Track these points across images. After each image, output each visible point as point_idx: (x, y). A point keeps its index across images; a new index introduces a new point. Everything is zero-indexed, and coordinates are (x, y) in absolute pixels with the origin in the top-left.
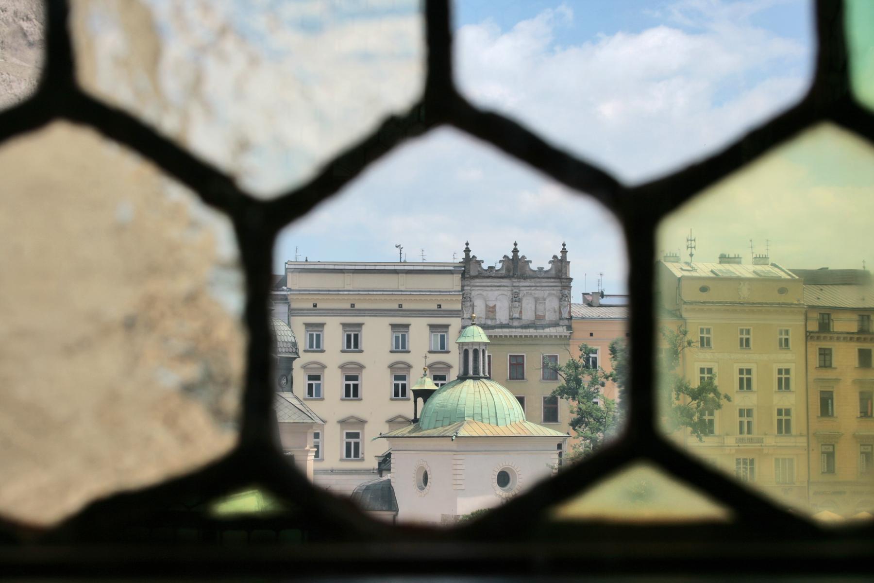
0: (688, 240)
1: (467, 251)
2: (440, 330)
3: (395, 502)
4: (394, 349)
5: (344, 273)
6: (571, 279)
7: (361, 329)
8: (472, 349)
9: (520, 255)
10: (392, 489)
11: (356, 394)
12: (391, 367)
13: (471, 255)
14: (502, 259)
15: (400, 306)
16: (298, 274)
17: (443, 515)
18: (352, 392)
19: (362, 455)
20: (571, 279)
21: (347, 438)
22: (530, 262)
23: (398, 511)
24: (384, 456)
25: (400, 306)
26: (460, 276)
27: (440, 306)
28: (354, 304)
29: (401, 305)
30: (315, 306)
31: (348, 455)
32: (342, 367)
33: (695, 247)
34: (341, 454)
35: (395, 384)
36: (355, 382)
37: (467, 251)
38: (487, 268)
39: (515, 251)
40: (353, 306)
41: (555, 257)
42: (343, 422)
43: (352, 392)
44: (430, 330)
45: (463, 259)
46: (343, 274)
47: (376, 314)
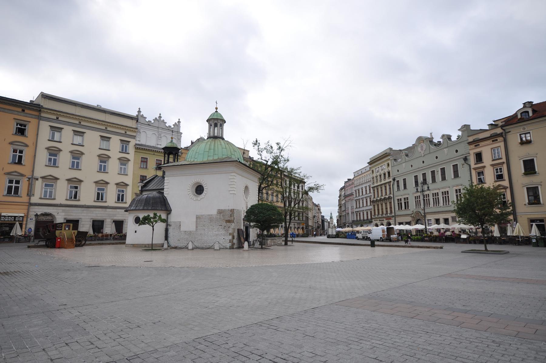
1: (139, 112)
2: (125, 143)
3: (168, 205)
5: (76, 106)
6: (181, 133)
9: (162, 119)
10: (165, 198)
12: (99, 156)
13: (141, 113)
15: (106, 128)
16: (48, 100)
18: (75, 166)
20: (181, 133)
22: (166, 123)
26: (136, 121)
27: (126, 132)
28: (81, 122)
36: (78, 161)
38: (147, 121)
39: (160, 117)
41: (176, 123)
43: (75, 166)
46: (75, 107)
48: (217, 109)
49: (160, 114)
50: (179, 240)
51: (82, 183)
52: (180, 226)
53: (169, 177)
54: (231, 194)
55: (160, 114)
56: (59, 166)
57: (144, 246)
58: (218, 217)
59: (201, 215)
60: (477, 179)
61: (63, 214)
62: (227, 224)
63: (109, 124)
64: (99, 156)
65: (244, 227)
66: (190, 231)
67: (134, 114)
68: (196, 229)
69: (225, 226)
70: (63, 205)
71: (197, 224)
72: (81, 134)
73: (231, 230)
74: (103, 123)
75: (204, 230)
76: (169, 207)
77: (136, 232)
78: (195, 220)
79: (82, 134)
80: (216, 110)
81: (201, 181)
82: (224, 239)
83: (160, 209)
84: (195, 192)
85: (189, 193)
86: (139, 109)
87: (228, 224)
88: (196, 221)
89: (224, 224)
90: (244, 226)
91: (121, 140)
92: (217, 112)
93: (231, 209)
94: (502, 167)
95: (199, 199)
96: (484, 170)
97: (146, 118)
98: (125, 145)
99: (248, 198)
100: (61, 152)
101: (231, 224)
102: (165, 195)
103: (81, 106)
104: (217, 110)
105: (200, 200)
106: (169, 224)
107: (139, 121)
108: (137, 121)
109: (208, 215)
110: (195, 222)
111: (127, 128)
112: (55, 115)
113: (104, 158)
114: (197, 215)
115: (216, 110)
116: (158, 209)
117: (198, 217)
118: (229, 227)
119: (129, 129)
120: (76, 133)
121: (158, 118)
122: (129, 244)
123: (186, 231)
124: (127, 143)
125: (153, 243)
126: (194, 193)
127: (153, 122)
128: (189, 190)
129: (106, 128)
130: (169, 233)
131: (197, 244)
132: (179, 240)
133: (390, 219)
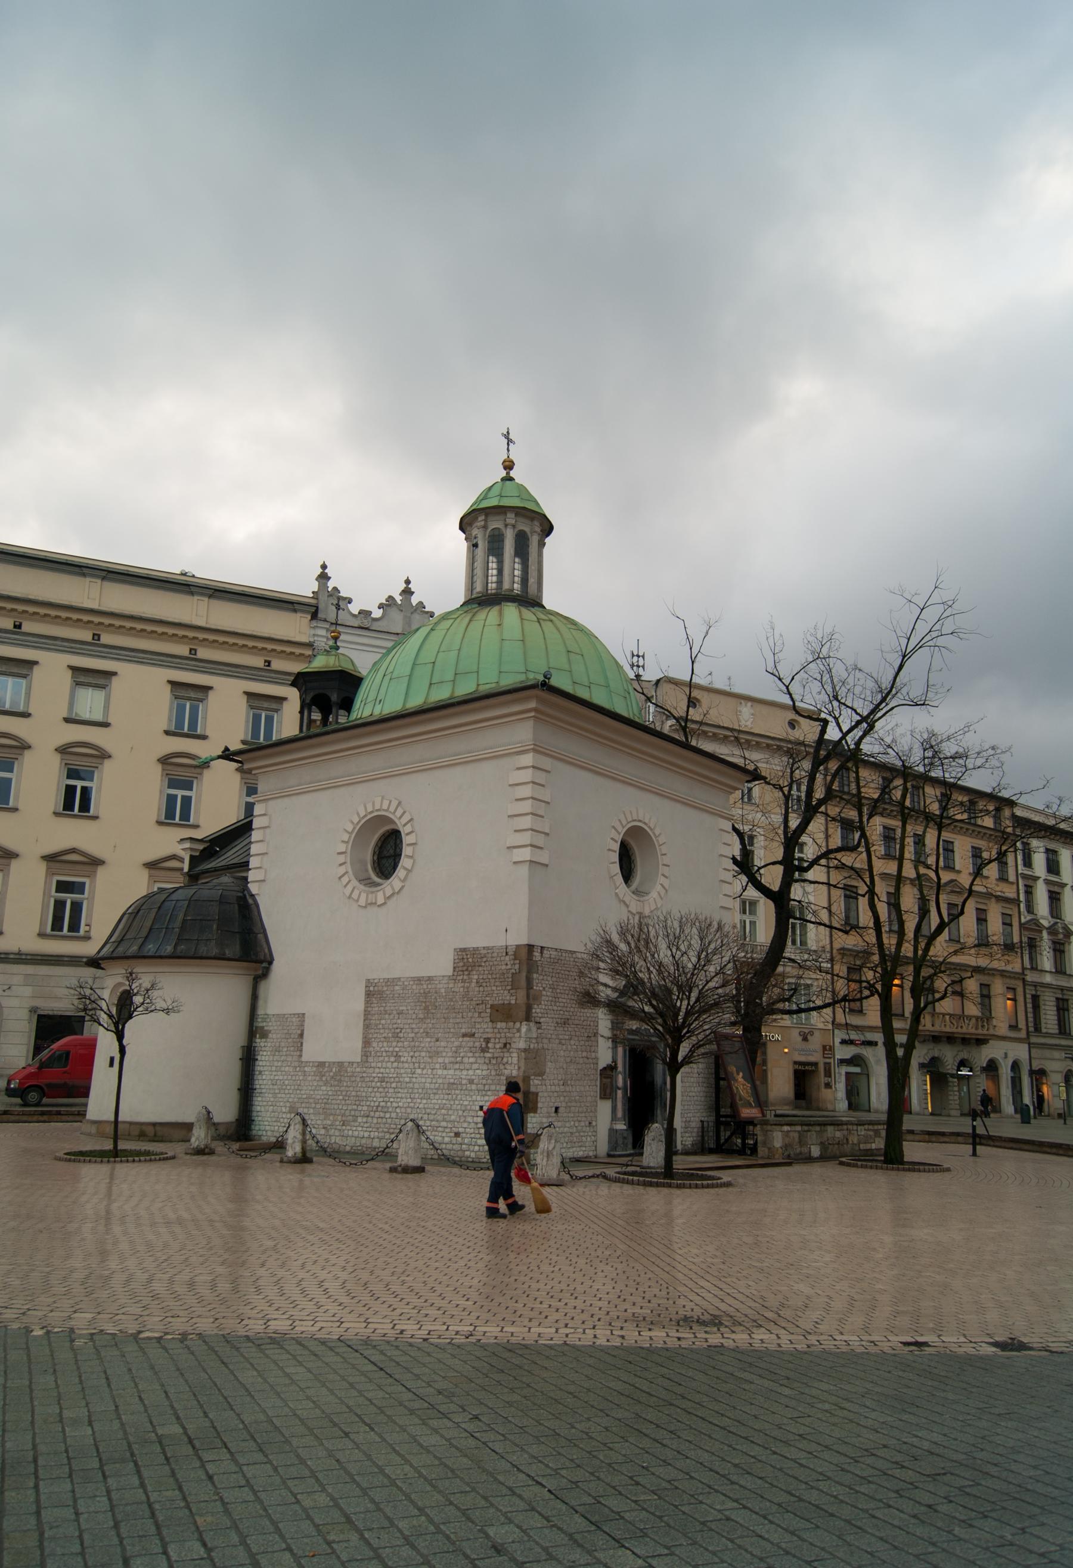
0: (633, 655)
1: (323, 577)
2: (266, 705)
4: (173, 728)
7: (110, 683)
8: (514, 526)
9: (414, 600)
10: (250, 901)
11: (85, 806)
12: (165, 761)
13: (331, 585)
14: (384, 602)
17: (464, 950)
19: (87, 928)
21: (56, 892)
23: (271, 963)
24: (206, 842)
25: (193, 652)
26: (309, 617)
29: (196, 650)
30: (18, 626)
31: (57, 924)
32: (63, 750)
33: (643, 667)
34: (42, 923)
35: (169, 795)
37: (323, 577)
38: (356, 613)
39: (407, 592)
40: (96, 638)
42: (51, 859)
44: (248, 702)
45: (313, 592)
47: (143, 658)
48: (509, 465)
49: (408, 582)
51: (101, 871)
52: (301, 1035)
53: (271, 803)
54: (515, 863)
55: (408, 582)
56: (100, 815)
57: (137, 1133)
58: (459, 987)
59: (387, 981)
61: (27, 991)
62: (499, 1025)
63: (201, 636)
64: (164, 761)
65: (620, 1050)
66: (341, 1064)
67: (305, 587)
68: (365, 1055)
69: (487, 1040)
70: (27, 955)
71: (367, 1027)
72: (100, 679)
73: (515, 1060)
74: (181, 632)
75: (397, 1056)
76: (265, 946)
78: (359, 1005)
79: (101, 682)
80: (504, 473)
81: (392, 809)
83: (215, 951)
84: (374, 869)
85: (342, 870)
86: (324, 567)
87: (503, 1025)
88: (367, 1014)
89: (485, 1027)
90: (615, 1040)
91: (250, 695)
92: (511, 479)
93: (518, 946)
95: (380, 900)
97: (350, 601)
98: (266, 716)
99: (654, 894)
100: (27, 753)
101: (518, 1025)
102: (253, 888)
103: (104, 574)
104: (512, 474)
105: (385, 903)
106: (263, 1027)
107: (320, 615)
108: (314, 616)
109: (414, 979)
111: (270, 646)
112: (10, 617)
113: (180, 769)
114: (368, 981)
115: (504, 473)
116: (204, 954)
117: (373, 993)
118: (505, 1045)
119: (279, 648)
120: (83, 677)
121: (398, 599)
123: (322, 1064)
124: (274, 706)
125: (120, 1119)
126: (367, 871)
127: (377, 613)
128: (342, 858)
129: (191, 650)
130: (260, 1072)
131: (366, 1134)
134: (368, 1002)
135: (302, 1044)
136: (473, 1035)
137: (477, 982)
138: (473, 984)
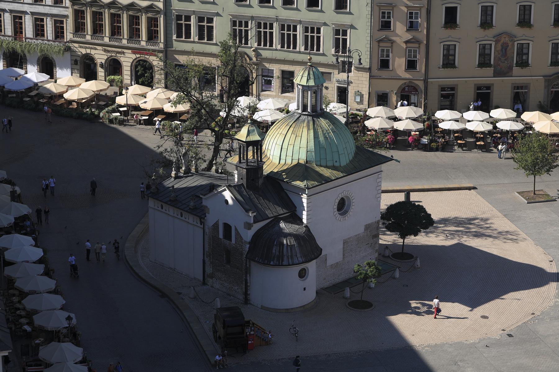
50: (324, 279)
52: (326, 260)
59: (349, 238)
60: (379, 22)
62: (374, 239)
66: (337, 263)
69: (372, 244)
71: (344, 251)
73: (377, 246)
77: (305, 289)
78: (342, 246)
82: (370, 259)
87: (375, 239)
88: (343, 248)
94: (419, 12)
96: (393, 10)
110: (342, 249)
122: (297, 308)
131: (344, 276)
132: (324, 279)
133: (151, 55)
134: (344, 245)
135: (326, 262)
136: (368, 244)
137: (370, 232)
138: (369, 232)
